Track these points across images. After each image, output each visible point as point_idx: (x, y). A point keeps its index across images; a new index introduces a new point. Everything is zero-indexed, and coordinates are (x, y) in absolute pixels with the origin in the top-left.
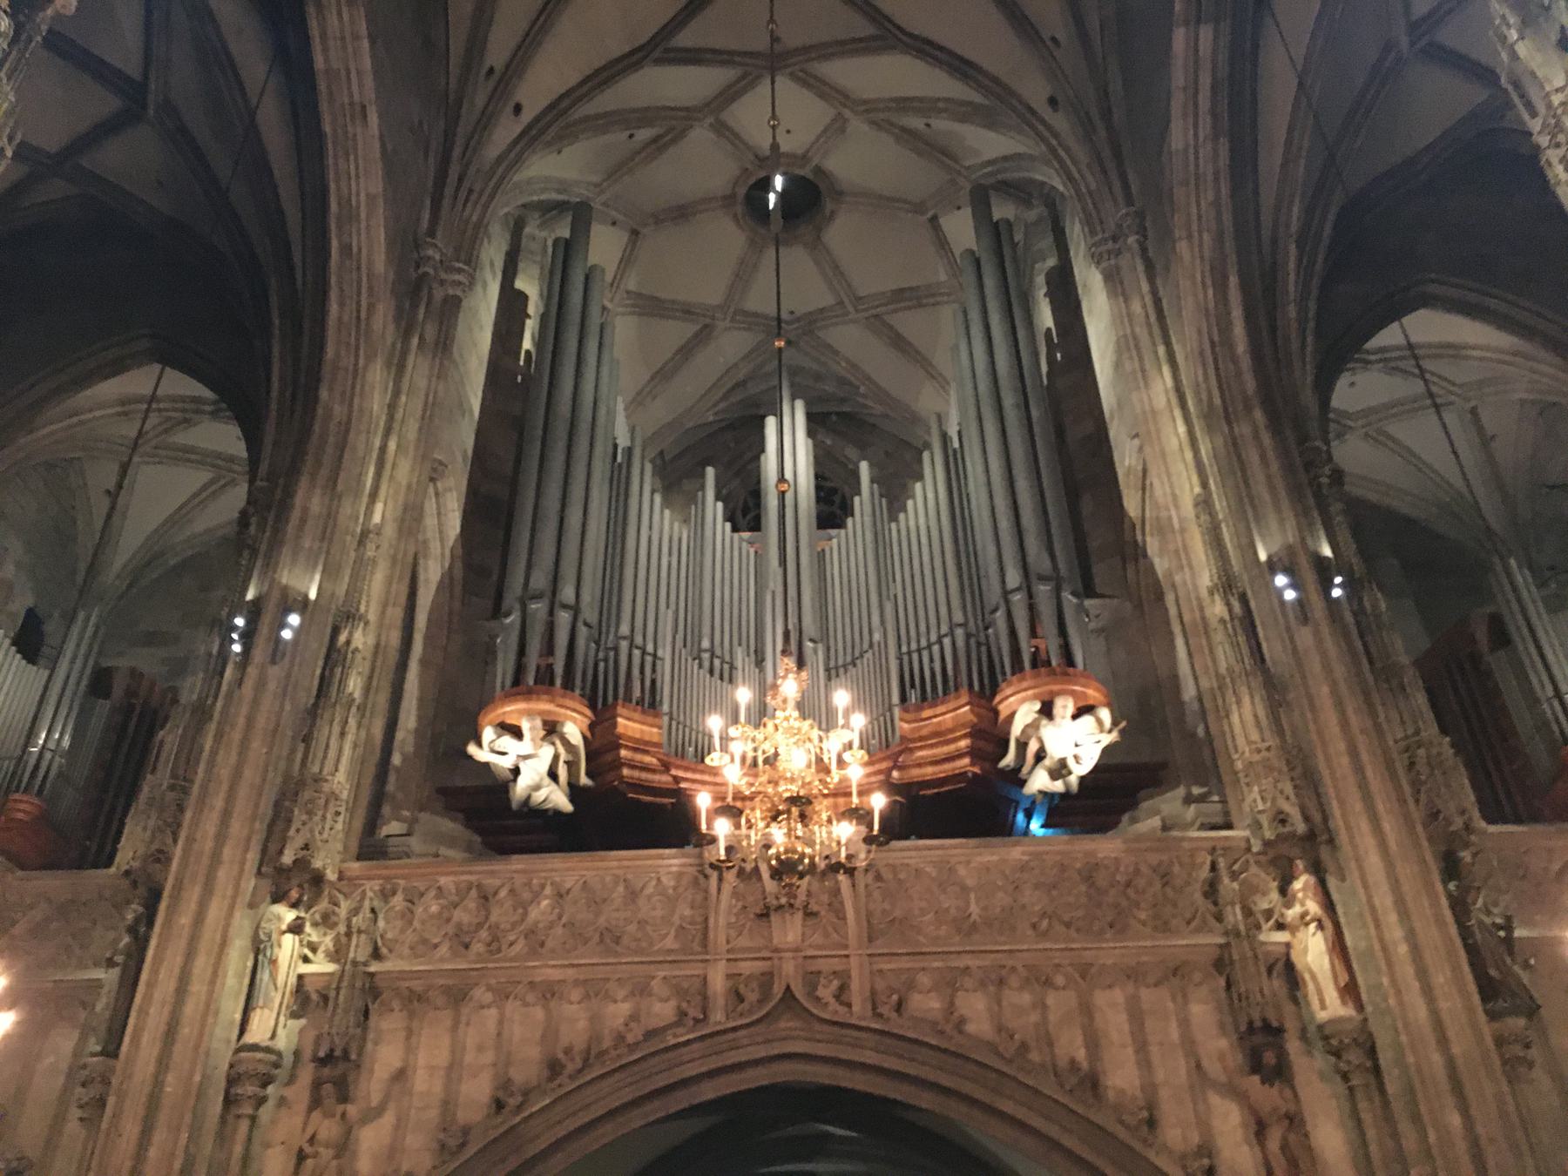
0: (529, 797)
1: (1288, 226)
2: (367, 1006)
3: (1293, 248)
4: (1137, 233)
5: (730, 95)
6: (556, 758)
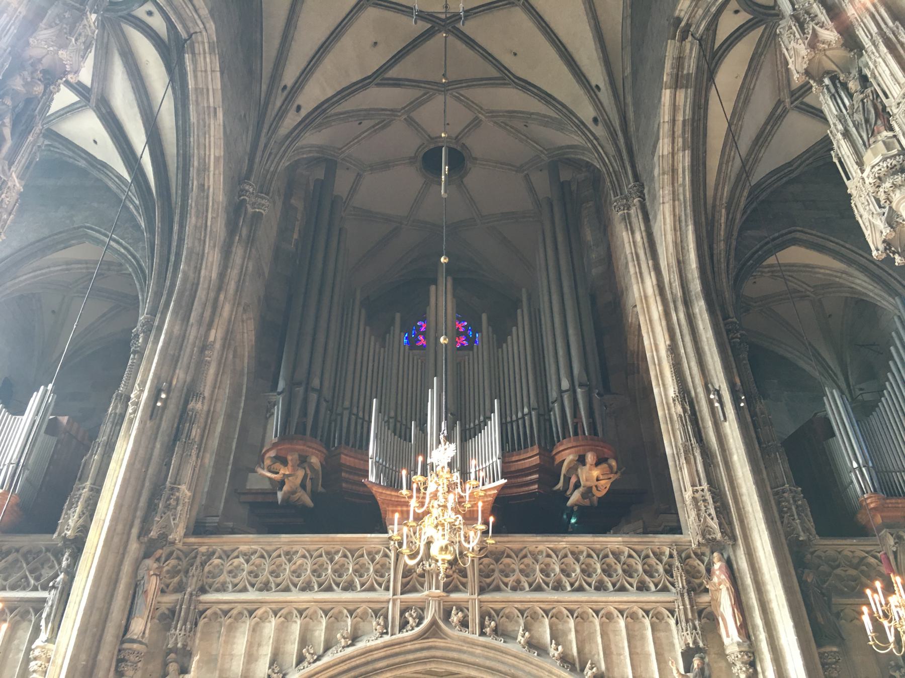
0: (289, 497)
1: (721, 199)
2: (196, 619)
3: (723, 211)
4: (639, 197)
5: (416, 104)
6: (305, 477)
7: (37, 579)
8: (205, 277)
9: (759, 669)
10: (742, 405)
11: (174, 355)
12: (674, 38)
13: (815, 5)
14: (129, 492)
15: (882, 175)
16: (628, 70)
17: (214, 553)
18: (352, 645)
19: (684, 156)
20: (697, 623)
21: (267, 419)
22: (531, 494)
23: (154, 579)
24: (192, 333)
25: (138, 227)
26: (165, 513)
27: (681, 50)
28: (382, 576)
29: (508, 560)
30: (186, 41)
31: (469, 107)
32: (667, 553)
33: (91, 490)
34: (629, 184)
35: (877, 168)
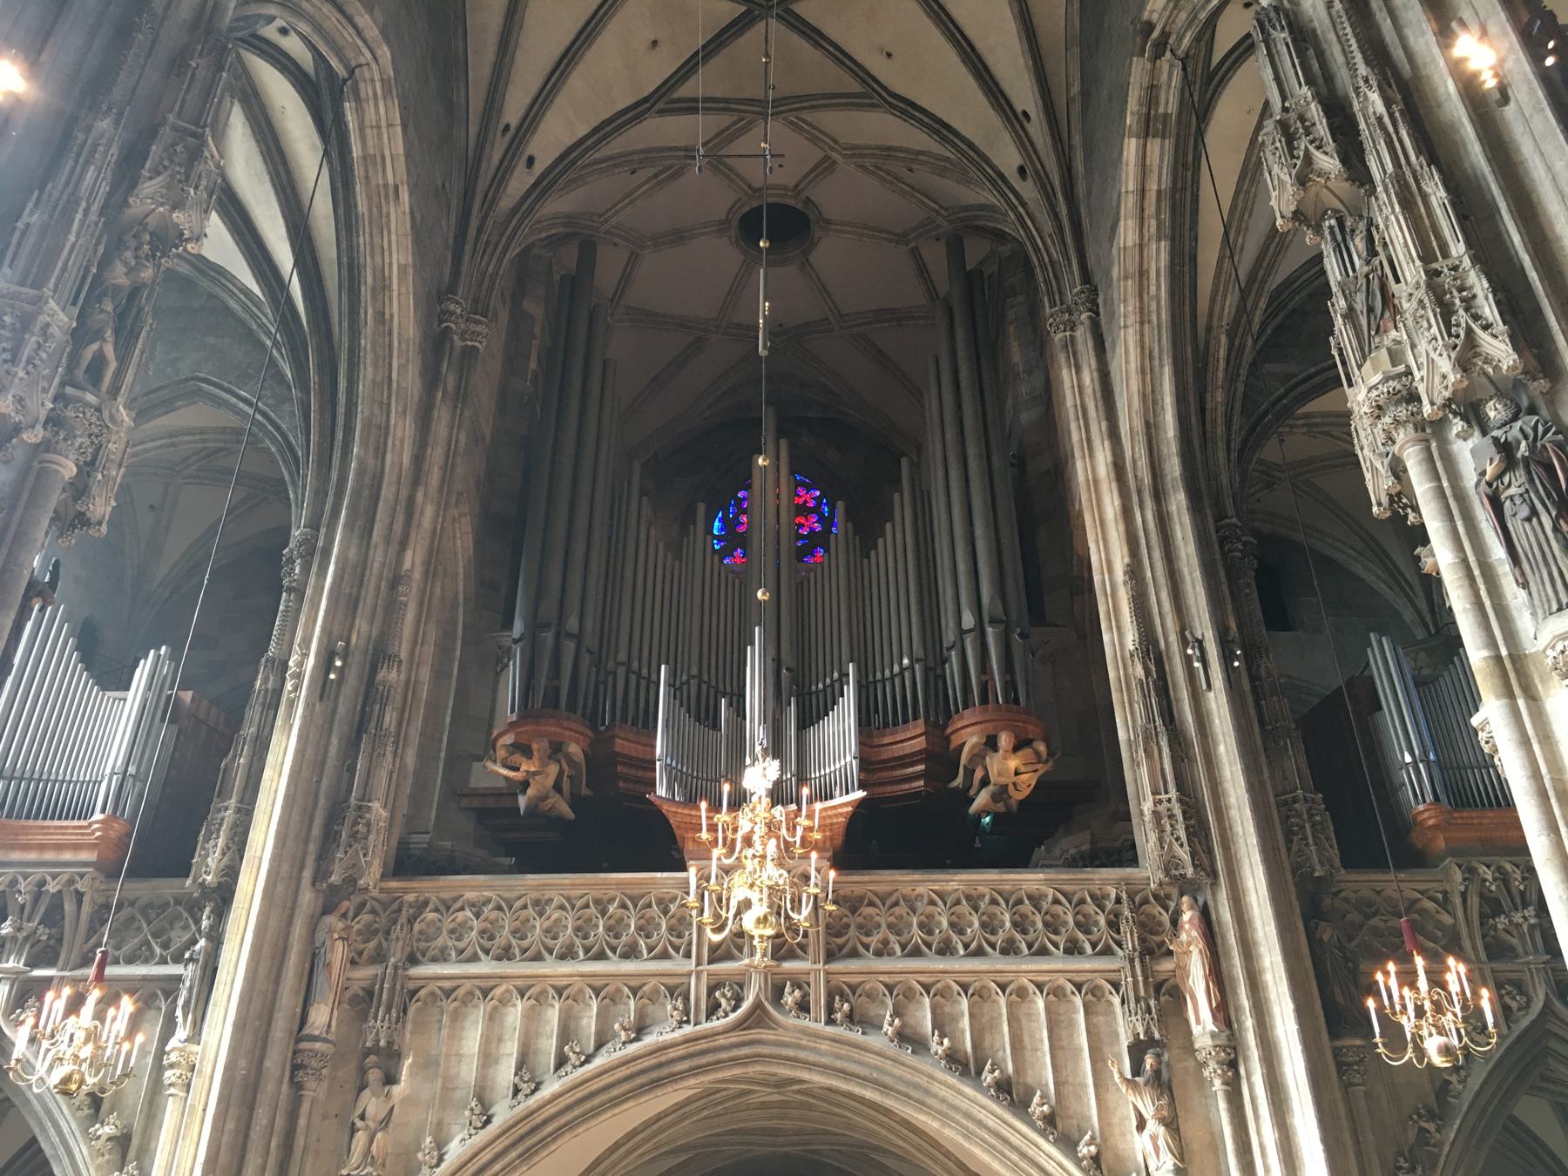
0: (536, 806)
1: (1220, 318)
3: (1223, 339)
4: (1090, 310)
6: (561, 773)
7: (165, 946)
8: (392, 464)
9: (1242, 1072)
10: (1236, 664)
11: (350, 594)
12: (1142, 54)
13: (1313, 106)
14: (296, 816)
15: (1381, 403)
16: (1075, 89)
17: (426, 903)
18: (637, 1039)
19: (1158, 250)
20: (1152, 1003)
21: (498, 674)
22: (916, 795)
23: (339, 944)
24: (377, 557)
25: (280, 377)
26: (351, 846)
27: (1153, 73)
28: (680, 936)
29: (870, 910)
30: (345, 81)
31: (814, 140)
32: (1113, 896)
33: (238, 811)
34: (1074, 288)
35: (1375, 393)
